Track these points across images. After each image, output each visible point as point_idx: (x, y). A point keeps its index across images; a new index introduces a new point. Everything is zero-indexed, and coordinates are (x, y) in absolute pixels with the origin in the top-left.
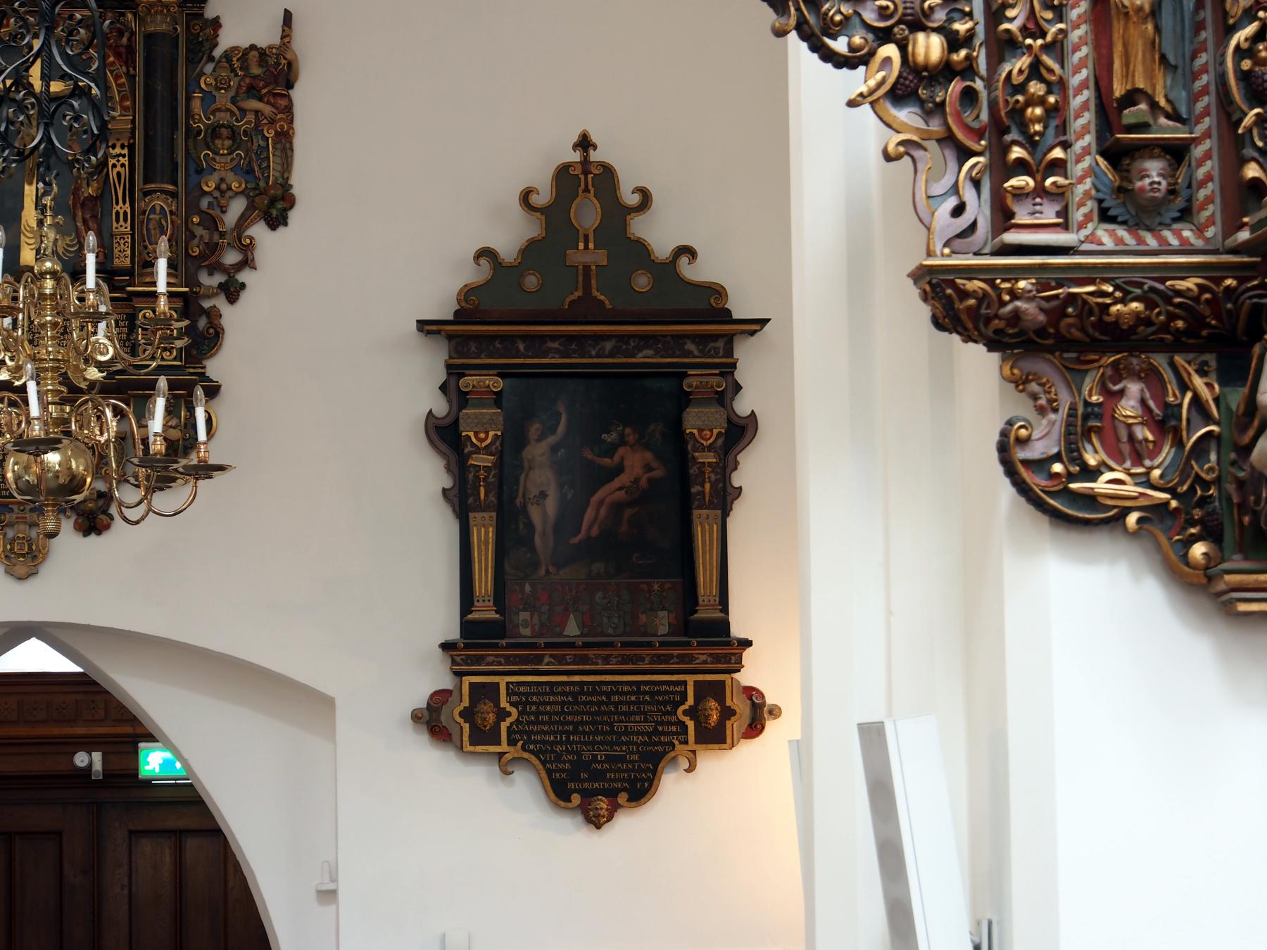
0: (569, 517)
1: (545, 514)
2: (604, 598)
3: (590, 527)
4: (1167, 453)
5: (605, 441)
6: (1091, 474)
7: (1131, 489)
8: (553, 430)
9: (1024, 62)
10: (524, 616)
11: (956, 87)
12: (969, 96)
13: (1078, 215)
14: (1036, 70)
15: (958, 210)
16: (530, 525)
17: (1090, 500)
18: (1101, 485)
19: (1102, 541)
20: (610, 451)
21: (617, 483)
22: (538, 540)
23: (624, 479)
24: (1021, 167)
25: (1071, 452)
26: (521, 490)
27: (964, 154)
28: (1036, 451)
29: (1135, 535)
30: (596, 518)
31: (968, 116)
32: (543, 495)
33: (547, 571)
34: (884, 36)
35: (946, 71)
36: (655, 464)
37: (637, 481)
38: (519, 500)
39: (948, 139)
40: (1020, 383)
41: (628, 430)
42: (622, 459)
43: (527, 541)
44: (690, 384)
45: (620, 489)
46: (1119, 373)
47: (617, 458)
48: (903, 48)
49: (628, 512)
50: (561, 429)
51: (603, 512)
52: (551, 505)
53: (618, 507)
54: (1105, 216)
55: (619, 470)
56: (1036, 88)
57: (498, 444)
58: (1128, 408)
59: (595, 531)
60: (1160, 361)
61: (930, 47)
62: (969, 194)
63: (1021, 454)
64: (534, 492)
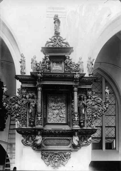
4: (33, 142)
6: (28, 143)
7: (30, 144)
9: (23, 116)
11: (20, 117)
12: (20, 118)
13: (27, 126)
14: (24, 117)
15: (19, 125)
17: (27, 144)
18: (28, 144)
19: (29, 147)
24: (23, 123)
25: (26, 141)
27: (20, 122)
28: (24, 141)
29: (31, 146)
31: (20, 119)
34: (15, 114)
35: (18, 116)
39: (19, 121)
40: (23, 137)
46: (29, 136)
48: (16, 115)
54: (29, 126)
56: (24, 118)
58: (30, 138)
60: (32, 135)
61: (18, 115)
62: (20, 124)
63: (23, 141)
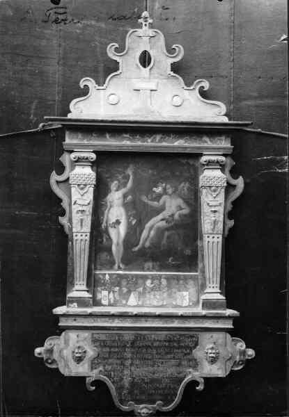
0: (133, 233)
1: (119, 233)
2: (152, 283)
3: (143, 244)
5: (154, 192)
8: (125, 185)
10: (105, 293)
16: (110, 239)
20: (159, 197)
21: (160, 217)
22: (114, 248)
23: (165, 214)
26: (105, 220)
30: (148, 236)
32: (118, 222)
33: (119, 266)
36: (183, 206)
37: (173, 215)
38: (103, 225)
41: (168, 186)
42: (165, 203)
43: (109, 250)
45: (162, 220)
47: (161, 201)
49: (166, 233)
50: (130, 184)
52: (122, 229)
53: (161, 232)
55: (162, 209)
57: (91, 206)
59: (147, 244)
64: (113, 220)
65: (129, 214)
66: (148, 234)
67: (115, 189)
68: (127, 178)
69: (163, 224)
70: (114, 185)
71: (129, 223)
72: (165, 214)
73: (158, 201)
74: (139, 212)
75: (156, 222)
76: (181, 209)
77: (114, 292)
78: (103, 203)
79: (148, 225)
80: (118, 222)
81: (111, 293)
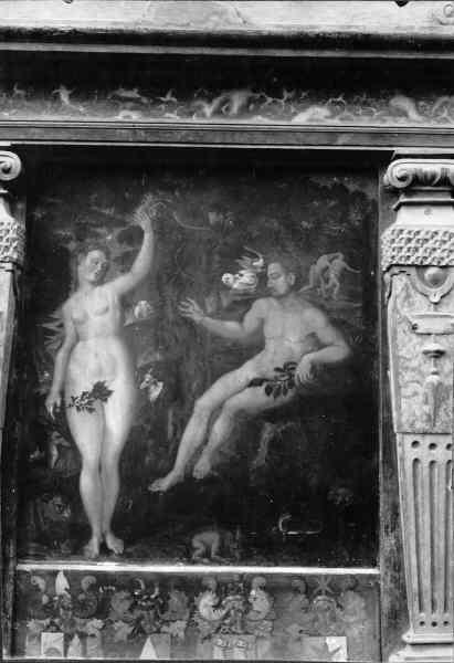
1: (104, 432)
2: (217, 607)
5: (227, 288)
8: (126, 261)
20: (244, 302)
21: (248, 371)
22: (86, 482)
23: (262, 365)
26: (58, 377)
30: (206, 441)
32: (101, 392)
36: (327, 334)
37: (289, 368)
41: (273, 268)
42: (262, 322)
44: (396, 171)
45: (254, 383)
47: (251, 320)
49: (268, 432)
51: (220, 429)
52: (117, 416)
53: (248, 425)
55: (254, 346)
59: (203, 467)
64: (83, 384)
65: (141, 363)
66: (203, 436)
67: (92, 277)
68: (134, 237)
69: (257, 398)
70: (89, 263)
71: (141, 395)
72: (262, 365)
73: (241, 320)
74: (176, 362)
75: (235, 390)
76: (320, 345)
77: (83, 636)
78: (51, 326)
79: (204, 403)
80: (101, 392)
81: (76, 640)
